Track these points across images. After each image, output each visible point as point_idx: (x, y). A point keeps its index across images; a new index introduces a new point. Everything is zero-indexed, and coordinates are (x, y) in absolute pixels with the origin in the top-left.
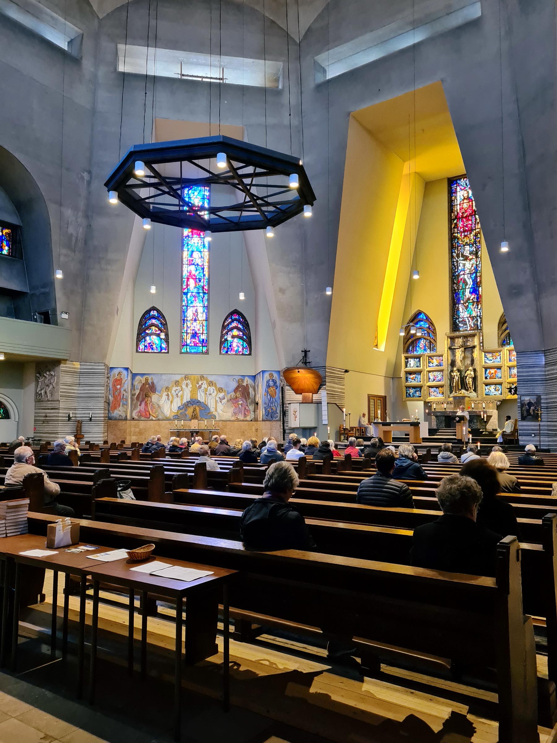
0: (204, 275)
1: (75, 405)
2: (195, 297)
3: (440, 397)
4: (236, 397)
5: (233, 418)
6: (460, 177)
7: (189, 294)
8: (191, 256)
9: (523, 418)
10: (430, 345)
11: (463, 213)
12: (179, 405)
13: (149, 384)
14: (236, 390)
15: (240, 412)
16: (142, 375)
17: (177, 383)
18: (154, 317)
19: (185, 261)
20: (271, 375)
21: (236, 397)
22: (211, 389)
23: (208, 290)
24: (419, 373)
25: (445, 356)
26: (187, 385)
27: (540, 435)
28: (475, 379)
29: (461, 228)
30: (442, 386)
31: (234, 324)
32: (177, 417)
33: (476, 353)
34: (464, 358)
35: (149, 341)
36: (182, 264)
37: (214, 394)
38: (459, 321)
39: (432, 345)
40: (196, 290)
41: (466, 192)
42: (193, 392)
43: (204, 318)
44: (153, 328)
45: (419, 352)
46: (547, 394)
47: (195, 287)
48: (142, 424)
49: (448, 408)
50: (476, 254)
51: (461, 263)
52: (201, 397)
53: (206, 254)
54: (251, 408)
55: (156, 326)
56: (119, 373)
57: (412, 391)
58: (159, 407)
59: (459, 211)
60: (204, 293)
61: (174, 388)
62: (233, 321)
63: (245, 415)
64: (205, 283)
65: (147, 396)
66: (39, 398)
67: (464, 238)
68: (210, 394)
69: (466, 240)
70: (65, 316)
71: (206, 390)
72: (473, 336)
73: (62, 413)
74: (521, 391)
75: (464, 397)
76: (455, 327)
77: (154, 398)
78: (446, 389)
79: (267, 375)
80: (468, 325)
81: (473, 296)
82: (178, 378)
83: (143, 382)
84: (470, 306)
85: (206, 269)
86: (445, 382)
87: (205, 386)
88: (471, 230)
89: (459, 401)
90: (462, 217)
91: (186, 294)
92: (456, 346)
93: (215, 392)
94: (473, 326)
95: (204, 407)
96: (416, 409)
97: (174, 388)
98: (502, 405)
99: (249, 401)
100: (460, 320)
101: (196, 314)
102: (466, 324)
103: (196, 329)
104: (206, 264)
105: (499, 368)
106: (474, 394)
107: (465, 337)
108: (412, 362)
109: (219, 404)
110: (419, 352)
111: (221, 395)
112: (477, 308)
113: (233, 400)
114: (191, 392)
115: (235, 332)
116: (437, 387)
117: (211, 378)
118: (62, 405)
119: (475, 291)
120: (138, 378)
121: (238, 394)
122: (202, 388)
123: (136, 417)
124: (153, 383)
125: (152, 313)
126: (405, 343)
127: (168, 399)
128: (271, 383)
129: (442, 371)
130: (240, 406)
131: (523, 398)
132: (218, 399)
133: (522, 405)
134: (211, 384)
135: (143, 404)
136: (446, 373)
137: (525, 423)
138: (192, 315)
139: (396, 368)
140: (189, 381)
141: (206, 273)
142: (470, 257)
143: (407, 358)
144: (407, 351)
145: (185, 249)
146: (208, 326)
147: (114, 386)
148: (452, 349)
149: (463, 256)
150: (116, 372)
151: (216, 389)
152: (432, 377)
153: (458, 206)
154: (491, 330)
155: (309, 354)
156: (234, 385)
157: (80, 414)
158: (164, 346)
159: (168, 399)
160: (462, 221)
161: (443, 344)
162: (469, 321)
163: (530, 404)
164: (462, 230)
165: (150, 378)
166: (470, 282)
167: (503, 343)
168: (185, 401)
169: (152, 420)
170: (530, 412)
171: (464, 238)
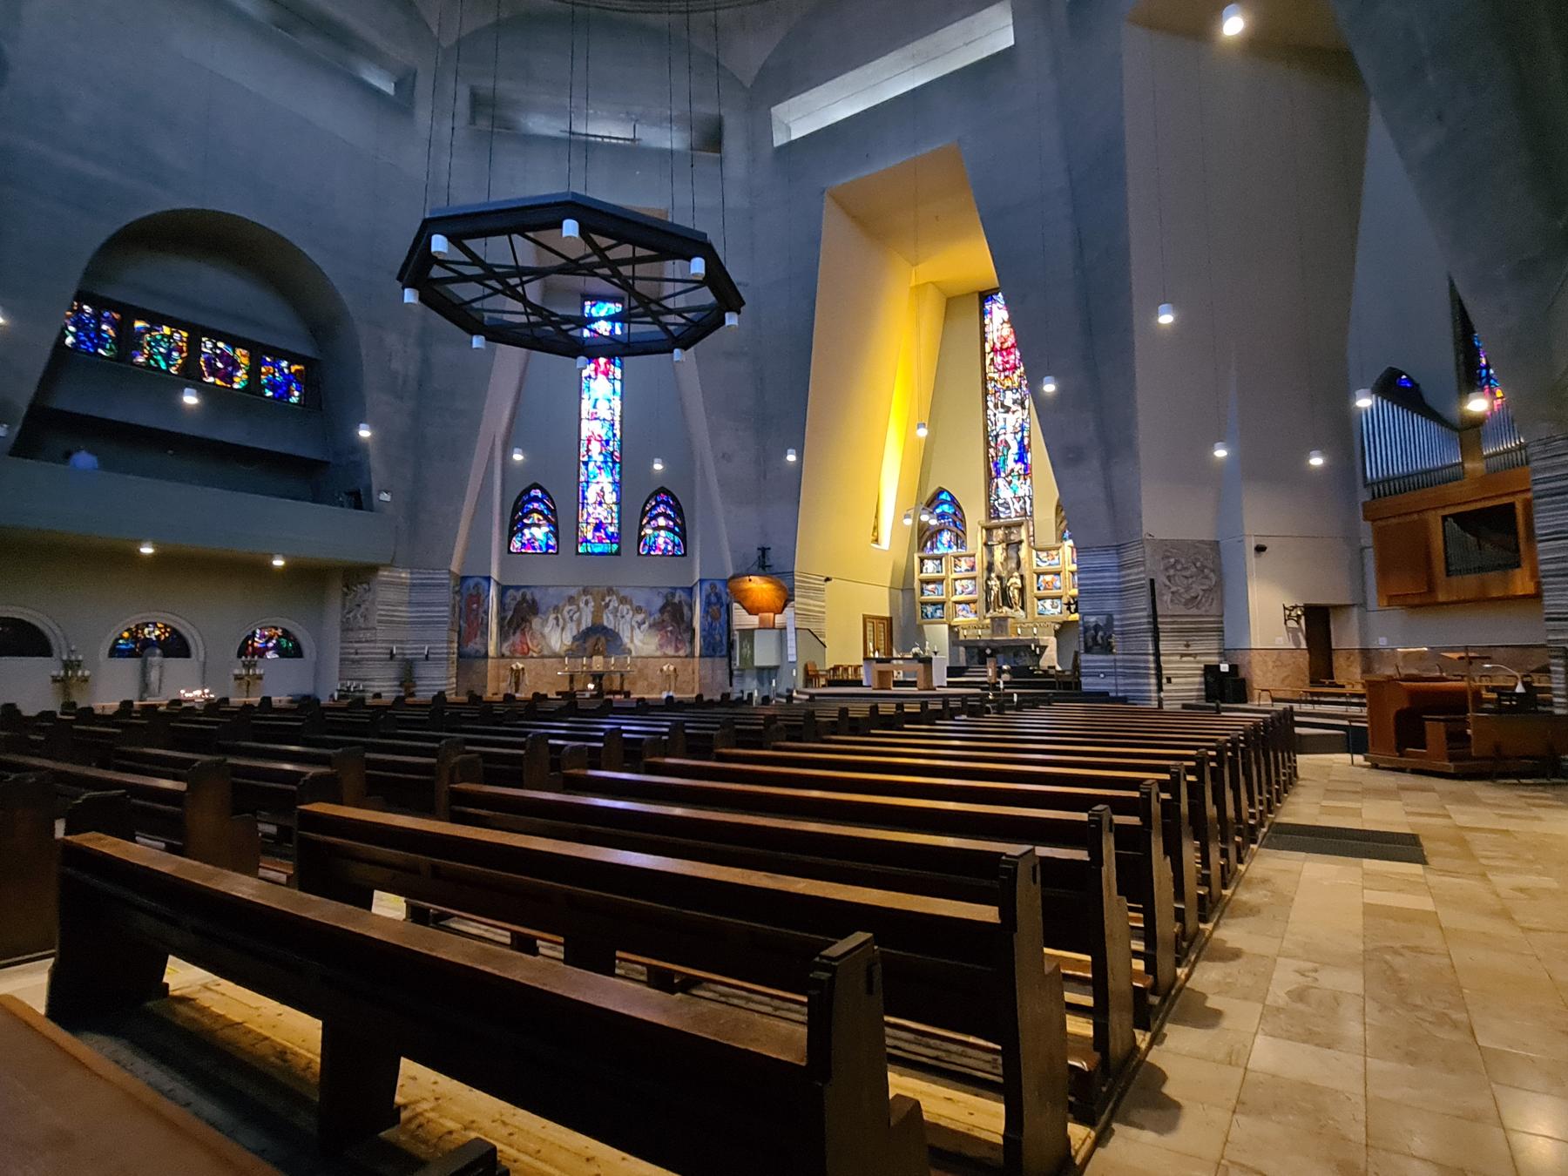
3: (972, 618)
5: (658, 653)
6: (995, 291)
7: (591, 465)
9: (1088, 650)
14: (662, 610)
15: (669, 642)
16: (517, 588)
17: (571, 600)
18: (536, 499)
19: (584, 414)
20: (713, 586)
22: (624, 608)
24: (940, 581)
25: (978, 555)
26: (587, 603)
27: (1116, 675)
28: (1022, 591)
30: (974, 602)
31: (661, 509)
32: (572, 653)
33: (1023, 552)
34: (1006, 559)
37: (628, 617)
39: (960, 540)
40: (601, 458)
42: (597, 614)
44: (536, 516)
45: (941, 550)
46: (1121, 612)
49: (984, 635)
50: (1022, 405)
51: (1001, 416)
52: (608, 621)
54: (687, 636)
55: (541, 513)
57: (930, 609)
58: (543, 636)
60: (614, 462)
61: (568, 608)
62: (658, 504)
63: (677, 649)
65: (524, 620)
66: (346, 628)
69: (1008, 383)
70: (385, 497)
71: (616, 609)
72: (1019, 525)
73: (380, 649)
74: (1084, 607)
75: (1006, 618)
76: (993, 513)
77: (536, 622)
78: (981, 605)
79: (706, 586)
82: (573, 592)
83: (519, 598)
84: (1015, 481)
86: (979, 595)
87: (614, 603)
89: (1000, 623)
91: (586, 464)
92: (995, 540)
96: (937, 637)
98: (1063, 630)
99: (683, 626)
101: (602, 493)
104: (617, 419)
105: (1058, 574)
106: (1022, 613)
107: (1008, 527)
108: (929, 565)
110: (941, 550)
111: (640, 617)
113: (658, 626)
115: (662, 522)
116: (968, 603)
118: (380, 636)
119: (1021, 458)
120: (511, 592)
121: (666, 616)
123: (507, 653)
124: (534, 601)
125: (533, 493)
126: (920, 538)
128: (713, 599)
129: (974, 578)
131: (1087, 618)
133: (1086, 630)
134: (623, 600)
136: (980, 581)
137: (1090, 657)
139: (909, 574)
141: (618, 433)
143: (922, 560)
144: (922, 548)
145: (585, 396)
146: (620, 512)
148: (988, 546)
149: (1003, 406)
152: (959, 589)
154: (1046, 516)
155: (771, 554)
156: (659, 602)
157: (410, 650)
158: (552, 542)
161: (975, 538)
163: (1097, 628)
166: (1015, 448)
167: (1062, 539)
168: (583, 627)
170: (1097, 639)
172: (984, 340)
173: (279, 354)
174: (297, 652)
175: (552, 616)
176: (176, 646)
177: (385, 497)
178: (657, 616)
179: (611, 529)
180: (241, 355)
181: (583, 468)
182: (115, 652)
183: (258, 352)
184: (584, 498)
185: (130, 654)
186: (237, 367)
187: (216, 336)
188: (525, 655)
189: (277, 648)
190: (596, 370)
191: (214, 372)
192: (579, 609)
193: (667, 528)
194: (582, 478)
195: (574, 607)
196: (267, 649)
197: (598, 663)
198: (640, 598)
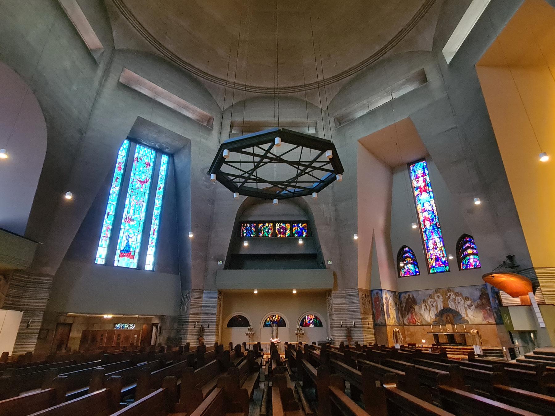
0: (435, 216)
1: (344, 317)
2: (432, 232)
4: (483, 304)
5: (485, 322)
8: (423, 206)
12: (436, 313)
13: (411, 299)
14: (481, 298)
15: (490, 316)
16: (406, 292)
17: (431, 296)
18: (407, 252)
19: (420, 211)
21: (483, 304)
22: (459, 298)
23: (440, 225)
26: (439, 297)
32: (436, 323)
35: (407, 269)
36: (418, 214)
40: (431, 228)
42: (445, 302)
43: (442, 245)
44: (408, 259)
47: (431, 225)
48: (412, 329)
52: (452, 305)
53: (433, 201)
55: (410, 257)
56: (377, 293)
58: (421, 315)
60: (438, 228)
61: (430, 300)
64: (437, 221)
68: (459, 303)
71: (454, 300)
77: (416, 308)
82: (431, 292)
85: (435, 211)
87: (453, 296)
91: (425, 232)
93: (463, 301)
95: (456, 314)
97: (430, 300)
101: (435, 244)
103: (438, 255)
104: (435, 208)
109: (469, 311)
111: (469, 303)
113: (480, 307)
114: (443, 302)
117: (457, 290)
120: (403, 295)
122: (451, 298)
123: (407, 323)
124: (413, 297)
127: (427, 309)
130: (489, 311)
132: (466, 306)
134: (457, 294)
135: (410, 313)
138: (432, 245)
140: (439, 294)
141: (436, 214)
145: (418, 203)
147: (375, 302)
150: (375, 292)
151: (463, 298)
156: (478, 294)
159: (427, 309)
165: (411, 294)
168: (439, 309)
169: (418, 325)
173: (298, 222)
174: (321, 325)
175: (423, 305)
176: (281, 323)
177: (330, 262)
178: (479, 301)
179: (444, 259)
180: (288, 226)
181: (424, 234)
182: (265, 325)
183: (291, 223)
184: (428, 247)
185: (270, 326)
186: (286, 229)
187: (279, 222)
188: (415, 324)
189: (313, 323)
190: (420, 191)
191: (280, 233)
192: (435, 301)
193: (473, 254)
194: (425, 239)
195: (432, 300)
196: (310, 323)
197: (449, 329)
198: (466, 292)
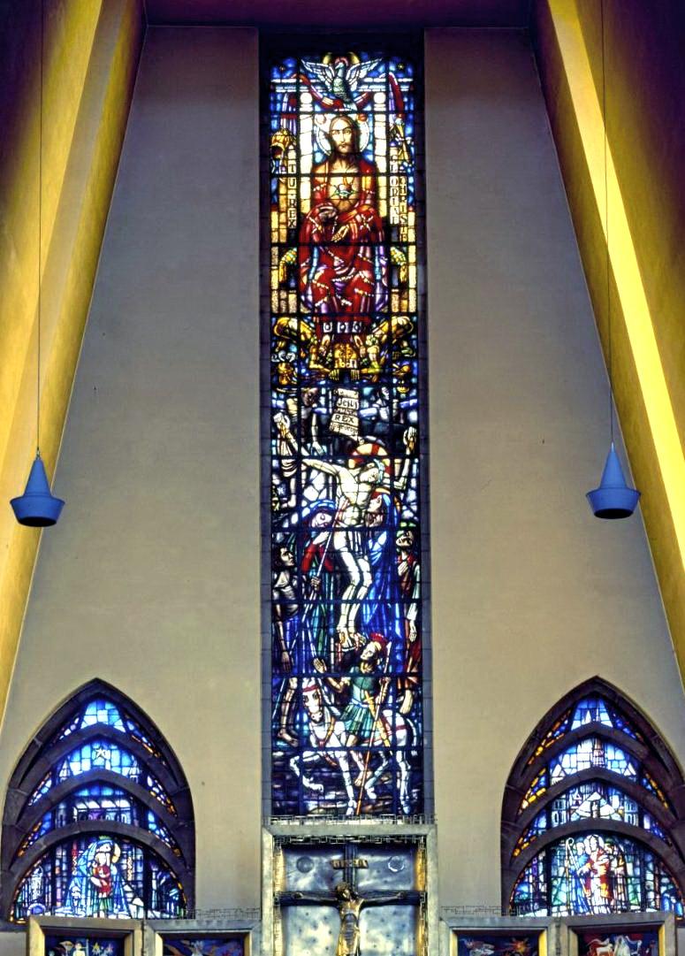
10: (147, 875)
11: (327, 222)
29: (317, 296)
38: (300, 764)
41: (341, 124)
59: (306, 207)
67: (331, 347)
69: (345, 359)
80: (350, 790)
81: (373, 647)
88: (370, 317)
90: (325, 240)
94: (373, 796)
100: (308, 756)
102: (338, 784)
112: (396, 708)
142: (365, 449)
149: (326, 435)
153: (306, 183)
160: (324, 259)
162: (354, 771)
164: (322, 305)
171: (331, 347)
172: (269, 202)
